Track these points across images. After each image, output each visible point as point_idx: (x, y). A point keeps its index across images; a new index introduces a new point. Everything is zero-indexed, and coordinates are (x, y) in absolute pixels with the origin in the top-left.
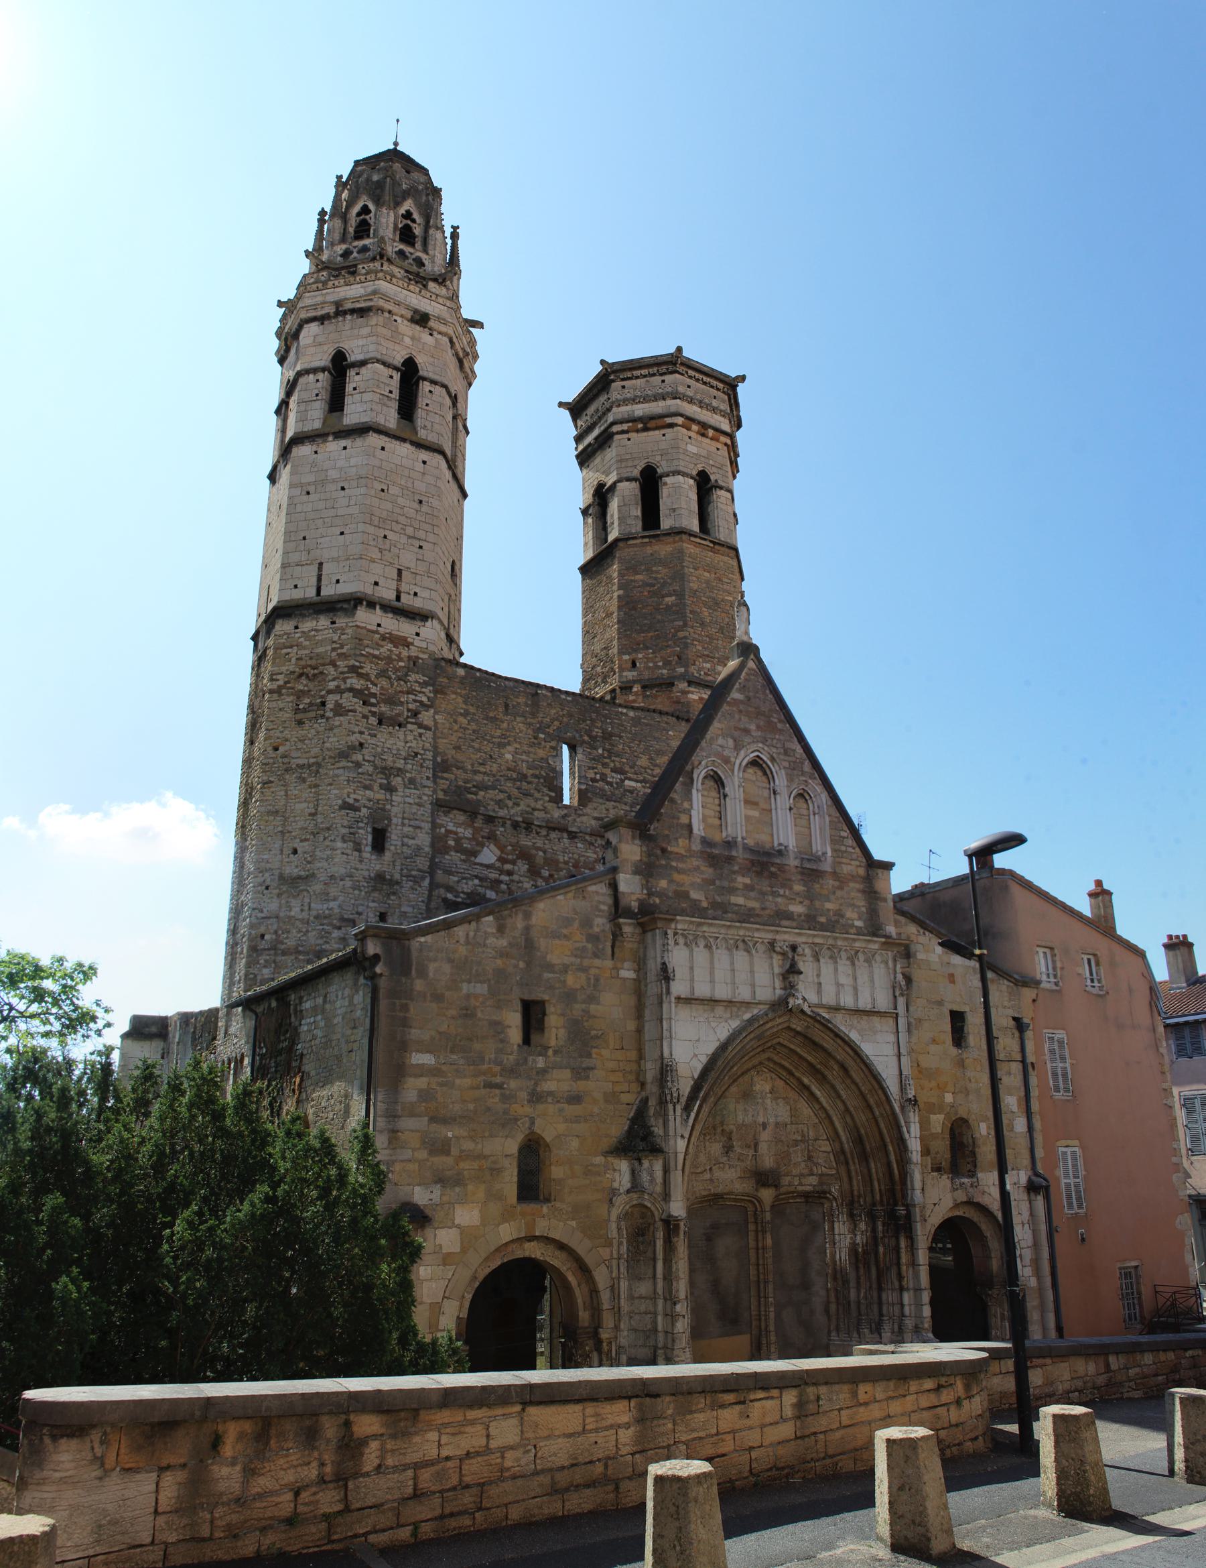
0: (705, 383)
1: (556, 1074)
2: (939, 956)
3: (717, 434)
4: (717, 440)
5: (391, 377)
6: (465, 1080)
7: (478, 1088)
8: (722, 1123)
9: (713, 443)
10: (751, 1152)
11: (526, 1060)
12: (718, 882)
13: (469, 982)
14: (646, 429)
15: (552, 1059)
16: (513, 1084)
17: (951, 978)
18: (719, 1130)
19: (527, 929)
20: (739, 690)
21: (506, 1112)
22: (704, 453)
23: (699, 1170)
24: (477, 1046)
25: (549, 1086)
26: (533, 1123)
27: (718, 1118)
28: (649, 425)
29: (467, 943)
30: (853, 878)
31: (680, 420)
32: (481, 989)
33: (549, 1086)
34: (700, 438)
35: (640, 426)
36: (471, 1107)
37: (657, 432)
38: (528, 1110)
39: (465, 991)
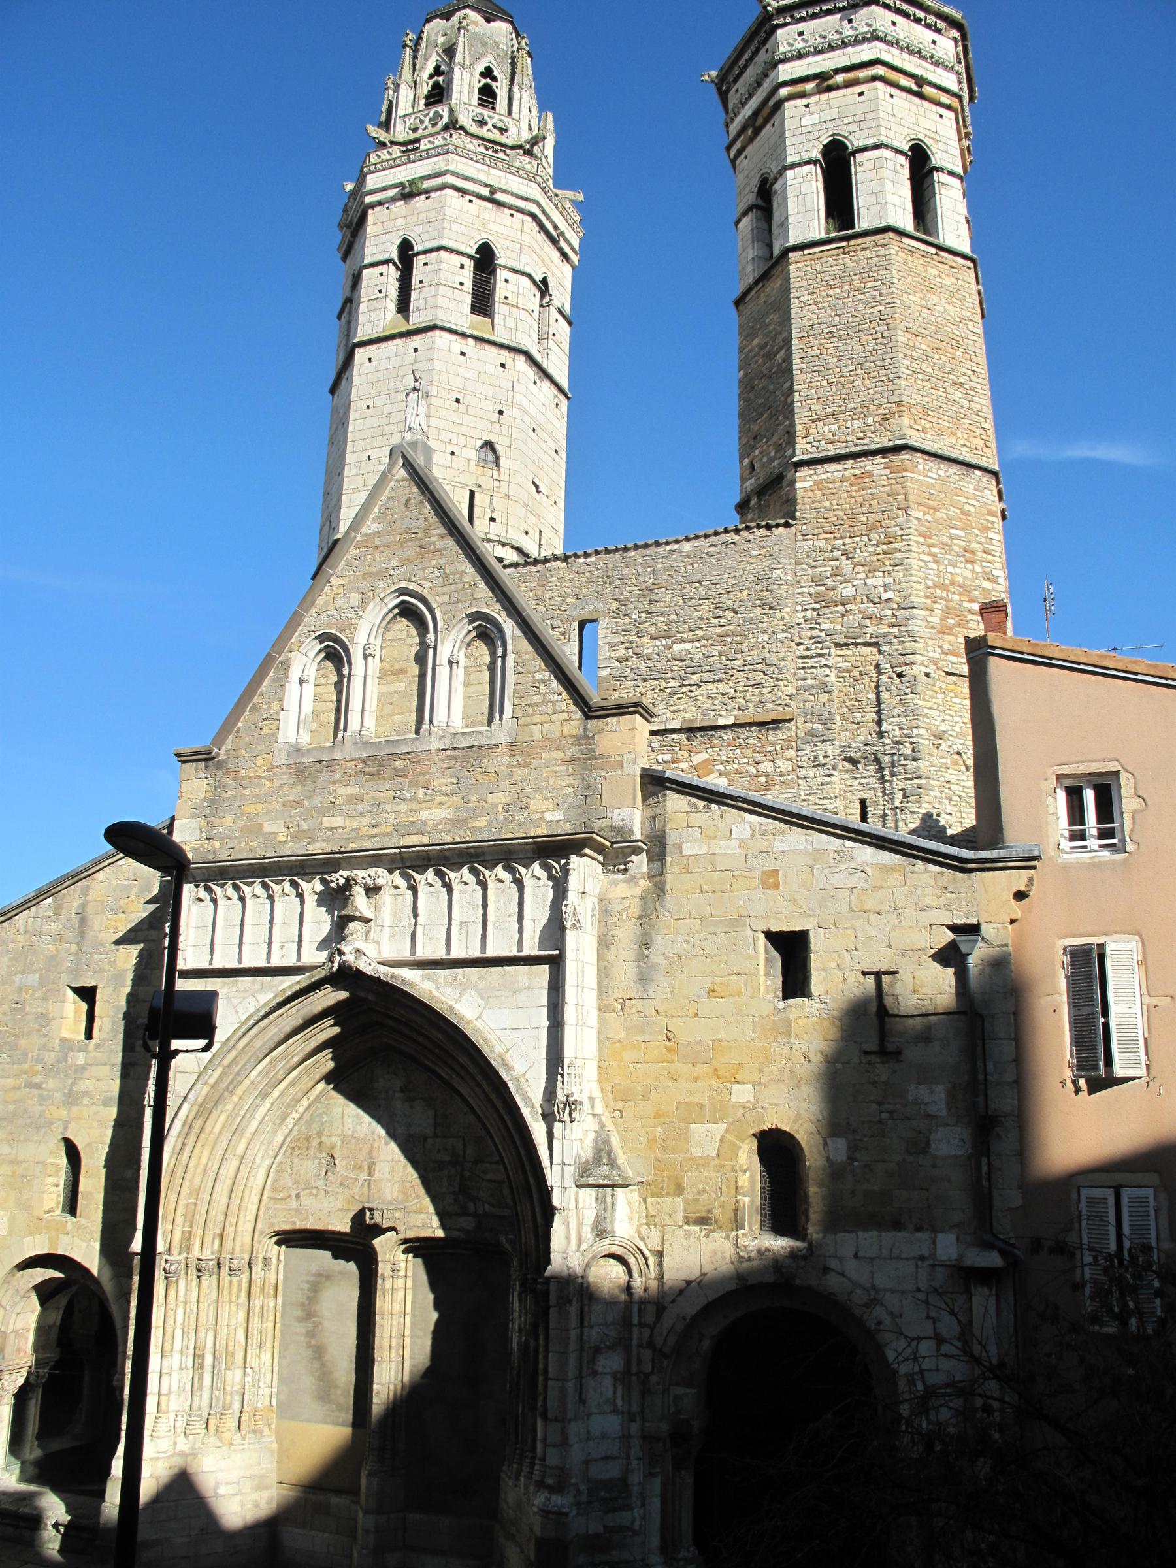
1: (96, 1071)
2: (743, 844)
6: (9, 1080)
7: (19, 1088)
8: (320, 1134)
9: (850, 90)
10: (363, 1175)
11: (66, 1056)
12: (306, 803)
13: (23, 973)
14: (757, 131)
15: (93, 1054)
16: (52, 1084)
17: (771, 880)
18: (315, 1143)
19: (83, 906)
20: (378, 519)
21: (42, 1115)
23: (281, 1195)
24: (23, 1042)
25: (85, 1085)
26: (66, 1128)
27: (315, 1128)
29: (26, 932)
30: (553, 742)
32: (33, 979)
33: (85, 1085)
34: (825, 96)
35: (750, 132)
36: (11, 1108)
37: (768, 126)
38: (63, 1113)
39: (17, 984)
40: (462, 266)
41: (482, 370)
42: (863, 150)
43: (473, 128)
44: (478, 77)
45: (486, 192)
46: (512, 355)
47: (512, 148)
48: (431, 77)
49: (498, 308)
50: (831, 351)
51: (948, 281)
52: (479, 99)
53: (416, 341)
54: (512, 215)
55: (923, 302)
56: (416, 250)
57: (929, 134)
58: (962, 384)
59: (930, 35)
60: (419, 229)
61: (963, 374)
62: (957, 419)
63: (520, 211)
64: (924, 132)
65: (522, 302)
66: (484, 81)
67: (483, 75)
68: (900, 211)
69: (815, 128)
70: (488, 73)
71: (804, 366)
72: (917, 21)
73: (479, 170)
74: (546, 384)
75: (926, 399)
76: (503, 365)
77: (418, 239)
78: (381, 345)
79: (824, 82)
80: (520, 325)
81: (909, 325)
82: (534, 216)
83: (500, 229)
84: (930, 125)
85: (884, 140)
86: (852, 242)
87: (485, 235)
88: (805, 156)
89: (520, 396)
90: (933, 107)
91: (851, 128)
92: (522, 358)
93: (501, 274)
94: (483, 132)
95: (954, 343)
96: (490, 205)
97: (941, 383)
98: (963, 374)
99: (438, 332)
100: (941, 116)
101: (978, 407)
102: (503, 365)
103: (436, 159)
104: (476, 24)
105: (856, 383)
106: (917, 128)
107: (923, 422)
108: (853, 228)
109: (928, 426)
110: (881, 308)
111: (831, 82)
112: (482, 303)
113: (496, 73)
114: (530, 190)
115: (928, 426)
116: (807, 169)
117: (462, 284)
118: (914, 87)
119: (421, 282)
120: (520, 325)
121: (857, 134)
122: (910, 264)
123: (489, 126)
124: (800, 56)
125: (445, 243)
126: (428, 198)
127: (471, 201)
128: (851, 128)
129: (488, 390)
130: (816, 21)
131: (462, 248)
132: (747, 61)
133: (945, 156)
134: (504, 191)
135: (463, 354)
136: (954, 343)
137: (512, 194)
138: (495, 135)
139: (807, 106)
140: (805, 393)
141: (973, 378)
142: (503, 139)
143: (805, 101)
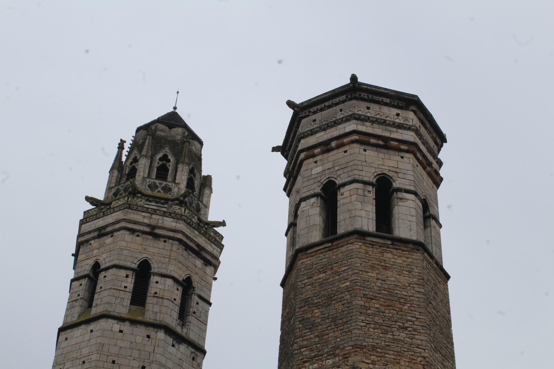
0: (329, 107)
3: (340, 141)
4: (343, 145)
5: (81, 285)
22: (330, 165)
28: (294, 175)
31: (302, 156)
34: (326, 155)
40: (127, 276)
41: (134, 341)
42: (344, 185)
43: (149, 192)
44: (157, 160)
45: (147, 229)
46: (156, 330)
47: (172, 200)
48: (131, 163)
49: (150, 300)
50: (317, 315)
51: (399, 261)
52: (157, 173)
53: (92, 326)
54: (165, 242)
55: (379, 276)
56: (101, 268)
57: (392, 169)
58: (406, 328)
59: (395, 111)
60: (104, 256)
61: (408, 321)
62: (399, 354)
63: (170, 238)
64: (389, 168)
65: (167, 295)
66: (161, 163)
67: (160, 159)
68: (365, 221)
69: (319, 175)
70: (165, 158)
71: (301, 326)
72: (386, 104)
73: (144, 217)
74: (183, 347)
75: (377, 341)
76: (148, 337)
77: (103, 262)
78: (74, 329)
79: (326, 147)
80: (164, 310)
81: (367, 293)
82: (179, 240)
83: (156, 251)
84: (393, 164)
85: (357, 177)
86: (335, 243)
87: (145, 255)
88: (312, 192)
89: (158, 356)
90: (397, 153)
91: (338, 173)
92: (162, 331)
93: (154, 279)
94: (155, 193)
95: (402, 301)
96: (151, 237)
97: (390, 329)
98: (408, 321)
99: (104, 320)
100: (402, 157)
101: (419, 342)
102: (148, 337)
103: (118, 213)
104: (162, 130)
105: (330, 335)
106: (383, 167)
107: (372, 357)
108: (336, 233)
109: (376, 359)
110: (348, 284)
111: (329, 147)
112: (139, 297)
113: (170, 157)
114: (178, 225)
115: (376, 359)
116: (313, 200)
117: (126, 287)
118: (381, 143)
119: (101, 288)
120: (164, 310)
121: (341, 176)
122: (370, 253)
123: (159, 189)
124: (313, 133)
125: (116, 262)
126: (112, 236)
127: (138, 236)
128: (338, 173)
129: (136, 354)
130: (323, 113)
131: (128, 264)
132: (292, 138)
133: (403, 181)
134: (160, 228)
135: (121, 331)
136: (402, 301)
137: (164, 228)
138: (162, 194)
139: (316, 162)
140: (301, 343)
141: (416, 323)
142: (168, 196)
143: (315, 159)
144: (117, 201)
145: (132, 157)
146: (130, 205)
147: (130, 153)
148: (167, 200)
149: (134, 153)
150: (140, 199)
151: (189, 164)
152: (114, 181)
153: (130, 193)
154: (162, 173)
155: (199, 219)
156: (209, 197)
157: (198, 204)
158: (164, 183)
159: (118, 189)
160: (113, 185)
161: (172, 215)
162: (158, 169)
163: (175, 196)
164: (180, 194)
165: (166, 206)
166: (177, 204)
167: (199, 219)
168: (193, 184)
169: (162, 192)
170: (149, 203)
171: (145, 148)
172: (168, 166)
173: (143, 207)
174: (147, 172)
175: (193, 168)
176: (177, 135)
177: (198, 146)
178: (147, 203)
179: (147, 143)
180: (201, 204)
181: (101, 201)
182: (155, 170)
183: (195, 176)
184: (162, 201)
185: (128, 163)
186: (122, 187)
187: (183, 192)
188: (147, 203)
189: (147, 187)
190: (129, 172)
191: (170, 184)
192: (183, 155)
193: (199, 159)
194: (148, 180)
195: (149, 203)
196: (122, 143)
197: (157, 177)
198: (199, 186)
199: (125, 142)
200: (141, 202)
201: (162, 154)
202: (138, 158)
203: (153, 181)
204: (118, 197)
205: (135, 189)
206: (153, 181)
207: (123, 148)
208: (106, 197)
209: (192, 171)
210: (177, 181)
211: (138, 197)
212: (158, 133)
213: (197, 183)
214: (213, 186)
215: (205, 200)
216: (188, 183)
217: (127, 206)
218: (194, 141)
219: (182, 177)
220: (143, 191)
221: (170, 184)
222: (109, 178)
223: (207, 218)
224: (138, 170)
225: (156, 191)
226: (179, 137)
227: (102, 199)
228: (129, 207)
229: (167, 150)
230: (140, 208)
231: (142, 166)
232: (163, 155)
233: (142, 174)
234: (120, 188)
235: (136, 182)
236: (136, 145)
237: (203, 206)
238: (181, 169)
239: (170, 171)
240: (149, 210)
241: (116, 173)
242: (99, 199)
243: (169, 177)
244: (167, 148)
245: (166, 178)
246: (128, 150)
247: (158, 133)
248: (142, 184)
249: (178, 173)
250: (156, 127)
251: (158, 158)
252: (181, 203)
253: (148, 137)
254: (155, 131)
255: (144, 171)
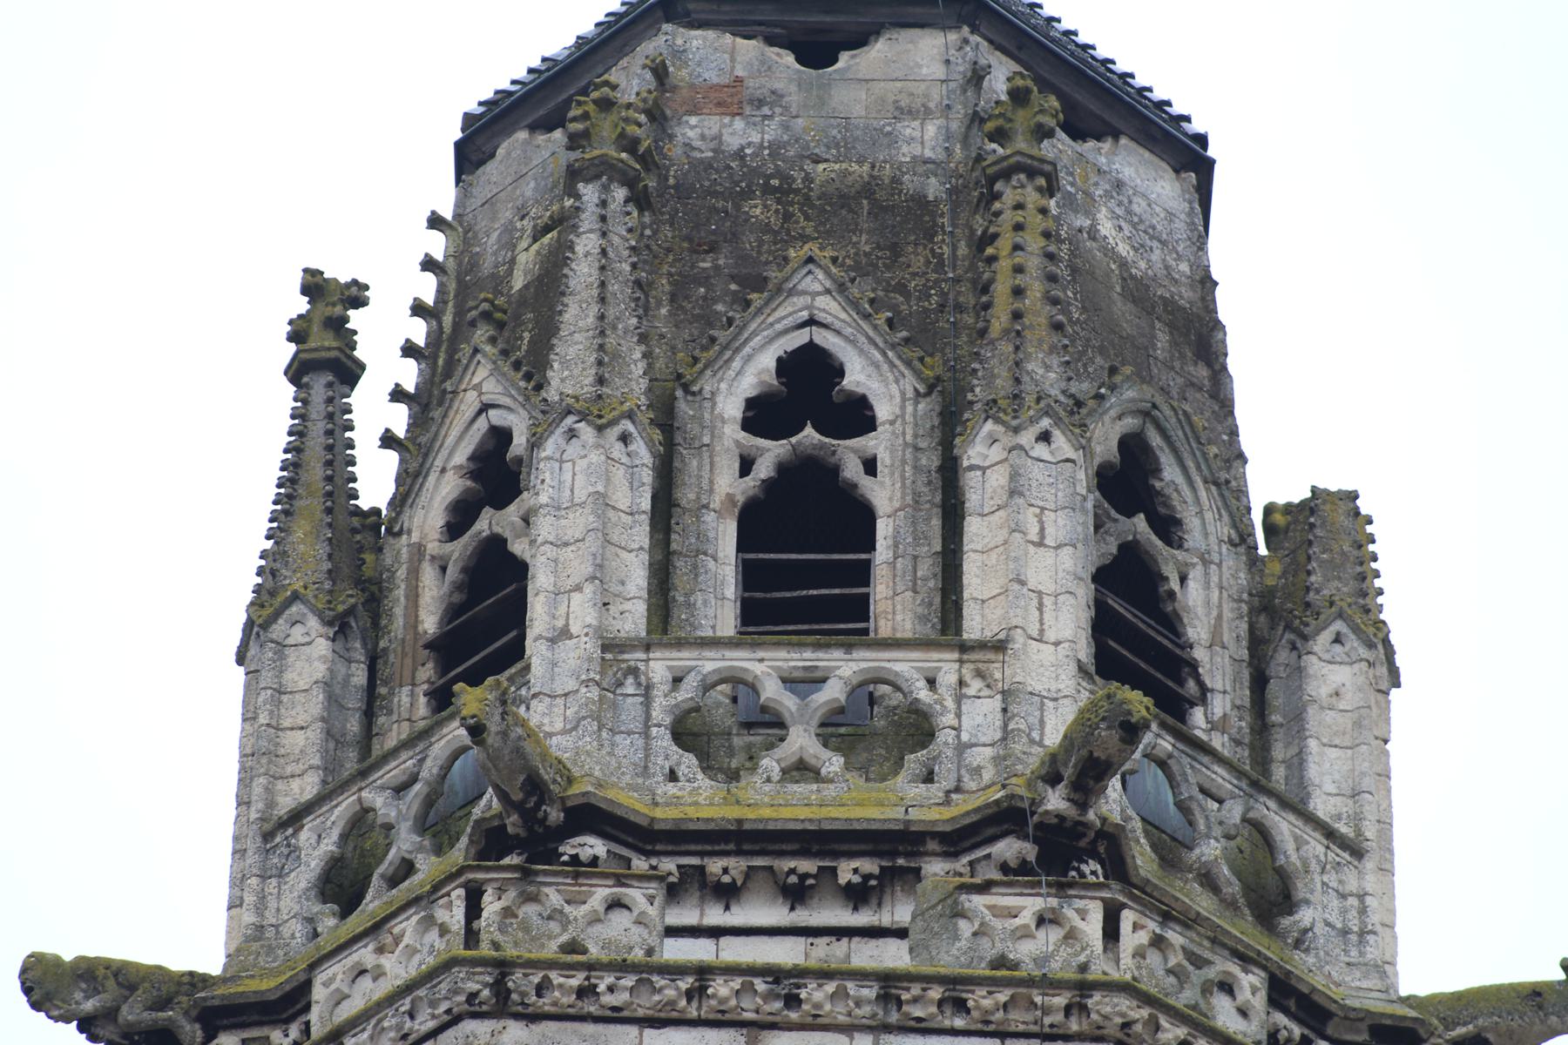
43: (696, 797)
44: (733, 434)
47: (957, 840)
48: (461, 517)
52: (751, 575)
66: (771, 453)
67: (763, 416)
70: (808, 392)
94: (765, 798)
104: (731, 98)
113: (858, 375)
123: (801, 741)
138: (845, 796)
142: (906, 799)
144: (365, 954)
145: (458, 445)
146: (503, 967)
147: (425, 404)
148: (896, 851)
149: (470, 402)
150: (601, 894)
151: (1076, 415)
152: (303, 743)
153: (492, 843)
154: (805, 555)
155: (1283, 991)
156: (1371, 731)
157: (1262, 833)
158: (844, 668)
159: (361, 820)
160: (306, 787)
161: (980, 999)
162: (755, 523)
163: (982, 788)
164: (1032, 761)
165: (900, 912)
166: (1017, 874)
167: (1283, 991)
168: (1172, 624)
169: (833, 763)
170: (715, 916)
171: (577, 317)
172: (852, 470)
173: (648, 970)
174: (635, 574)
175: (1134, 449)
176: (903, 112)
177: (1162, 189)
178: (685, 915)
179: (582, 272)
180: (1284, 827)
181: (195, 981)
182: (726, 536)
183: (1168, 527)
184: (847, 872)
185: (429, 518)
186: (400, 789)
187: (1055, 728)
188: (685, 915)
189: (663, 740)
190: (452, 612)
191: (904, 665)
192: (999, 320)
193: (1200, 335)
194: (659, 667)
195: (715, 916)
196: (329, 306)
197: (762, 615)
198: (1235, 631)
199: (355, 295)
200: (622, 919)
201: (767, 361)
202: (519, 442)
203: (710, 663)
204: (374, 903)
205: (535, 785)
206: (710, 663)
207: (348, 372)
208: (251, 941)
209: (1126, 483)
210: (974, 625)
211: (581, 869)
212: (694, 131)
213: (1207, 605)
214: (1395, 610)
215: (1327, 775)
216: (1103, 625)
217: (478, 983)
218: (1098, 152)
219: (1032, 564)
220: (628, 799)
221: (904, 665)
222: (249, 717)
223: (1383, 969)
224: (541, 580)
225: (770, 764)
226: (924, 139)
227: (211, 962)
228: (501, 990)
229: (815, 305)
230: (616, 992)
231: (578, 523)
232: (785, 366)
233: (582, 612)
234: (377, 799)
235: (539, 715)
236: (485, 310)
237: (1316, 846)
238: (998, 479)
239: (883, 528)
240: (721, 988)
241: (311, 653)
242: (178, 961)
243: (880, 589)
244: (815, 281)
245: (860, 608)
246: (409, 374)
247: (694, 131)
248: (603, 716)
249: (973, 527)
250: (660, 72)
251: (731, 407)
252: (1064, 852)
253: (589, 193)
254: (656, 115)
255: (599, 574)
